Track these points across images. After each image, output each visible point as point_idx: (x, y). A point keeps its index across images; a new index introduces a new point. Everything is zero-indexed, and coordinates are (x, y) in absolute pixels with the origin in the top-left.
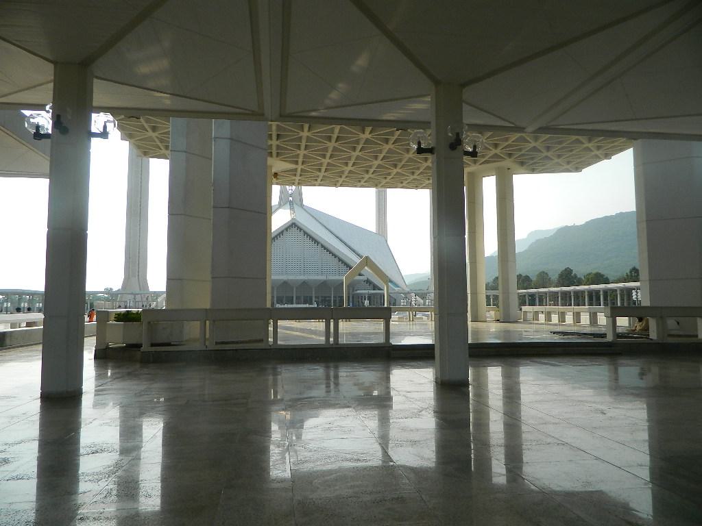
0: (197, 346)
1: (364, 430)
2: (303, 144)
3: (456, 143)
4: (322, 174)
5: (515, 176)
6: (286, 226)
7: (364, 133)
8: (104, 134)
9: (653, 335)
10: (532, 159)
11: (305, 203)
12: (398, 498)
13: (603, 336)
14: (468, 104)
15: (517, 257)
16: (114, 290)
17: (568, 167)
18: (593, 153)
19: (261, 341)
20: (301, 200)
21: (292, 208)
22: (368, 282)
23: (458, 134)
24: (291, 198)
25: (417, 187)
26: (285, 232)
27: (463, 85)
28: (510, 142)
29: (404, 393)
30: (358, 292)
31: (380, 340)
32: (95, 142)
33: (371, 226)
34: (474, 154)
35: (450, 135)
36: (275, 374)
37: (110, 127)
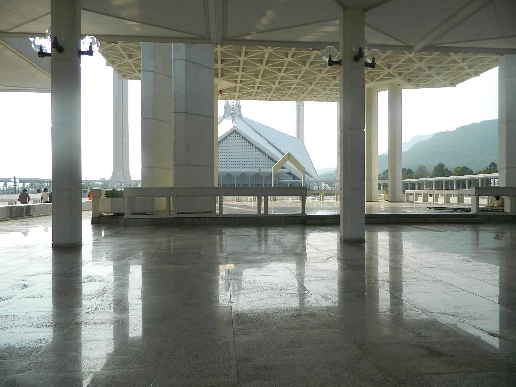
0: (165, 215)
1: (285, 270)
2: (241, 67)
3: (359, 56)
4: (255, 90)
5: (403, 91)
6: (230, 132)
8: (90, 53)
9: (508, 209)
10: (417, 76)
12: (311, 314)
13: (469, 209)
14: (369, 26)
16: (106, 180)
18: (465, 71)
19: (211, 212)
20: (240, 111)
21: (233, 119)
22: (290, 173)
23: (360, 49)
24: (232, 112)
25: (327, 100)
27: (366, 9)
28: (400, 63)
29: (316, 247)
30: (283, 181)
31: (300, 212)
32: (84, 58)
33: (292, 131)
34: (373, 65)
35: (354, 50)
36: (221, 233)
37: (95, 48)
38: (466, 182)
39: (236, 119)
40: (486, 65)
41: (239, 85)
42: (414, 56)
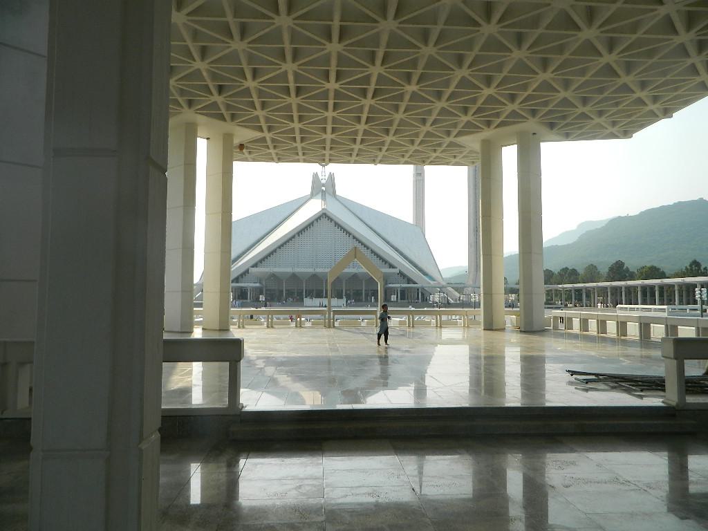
5: (543, 145)
6: (319, 215)
7: (329, 82)
10: (564, 117)
11: (338, 193)
13: (656, 385)
15: (544, 251)
17: (614, 130)
20: (334, 192)
21: (324, 198)
22: (401, 274)
24: (324, 188)
26: (315, 222)
28: (529, 92)
30: (390, 285)
33: (408, 216)
38: (657, 288)
39: (327, 200)
40: (683, 96)
41: (268, 136)
42: (552, 75)
